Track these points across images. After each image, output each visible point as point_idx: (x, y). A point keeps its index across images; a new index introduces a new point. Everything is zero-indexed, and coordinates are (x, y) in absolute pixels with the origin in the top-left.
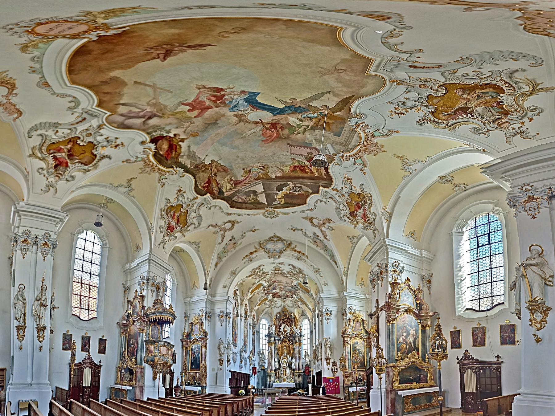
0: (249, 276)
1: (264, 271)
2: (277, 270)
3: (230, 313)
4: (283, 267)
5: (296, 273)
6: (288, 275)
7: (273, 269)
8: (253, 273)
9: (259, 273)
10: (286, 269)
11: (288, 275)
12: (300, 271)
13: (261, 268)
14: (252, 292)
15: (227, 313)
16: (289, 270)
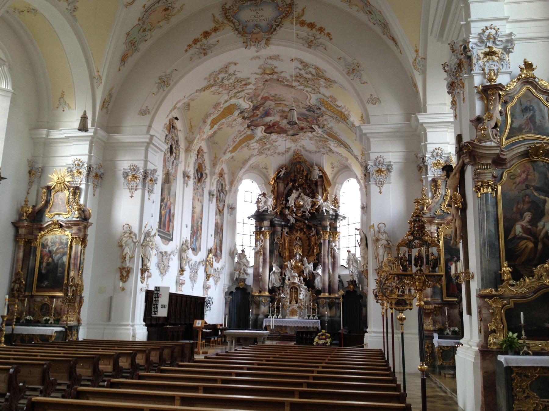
0: (204, 89)
1: (240, 75)
2: (270, 75)
3: (155, 171)
4: (280, 66)
5: (309, 76)
6: (294, 84)
7: (260, 71)
8: (214, 82)
9: (226, 82)
10: (288, 69)
11: (294, 84)
12: (319, 75)
13: (231, 70)
14: (214, 122)
15: (146, 172)
16: (294, 73)
